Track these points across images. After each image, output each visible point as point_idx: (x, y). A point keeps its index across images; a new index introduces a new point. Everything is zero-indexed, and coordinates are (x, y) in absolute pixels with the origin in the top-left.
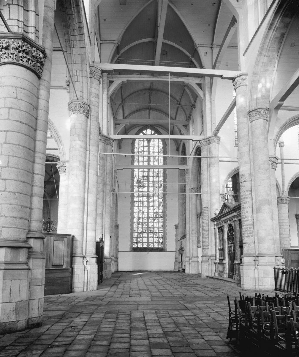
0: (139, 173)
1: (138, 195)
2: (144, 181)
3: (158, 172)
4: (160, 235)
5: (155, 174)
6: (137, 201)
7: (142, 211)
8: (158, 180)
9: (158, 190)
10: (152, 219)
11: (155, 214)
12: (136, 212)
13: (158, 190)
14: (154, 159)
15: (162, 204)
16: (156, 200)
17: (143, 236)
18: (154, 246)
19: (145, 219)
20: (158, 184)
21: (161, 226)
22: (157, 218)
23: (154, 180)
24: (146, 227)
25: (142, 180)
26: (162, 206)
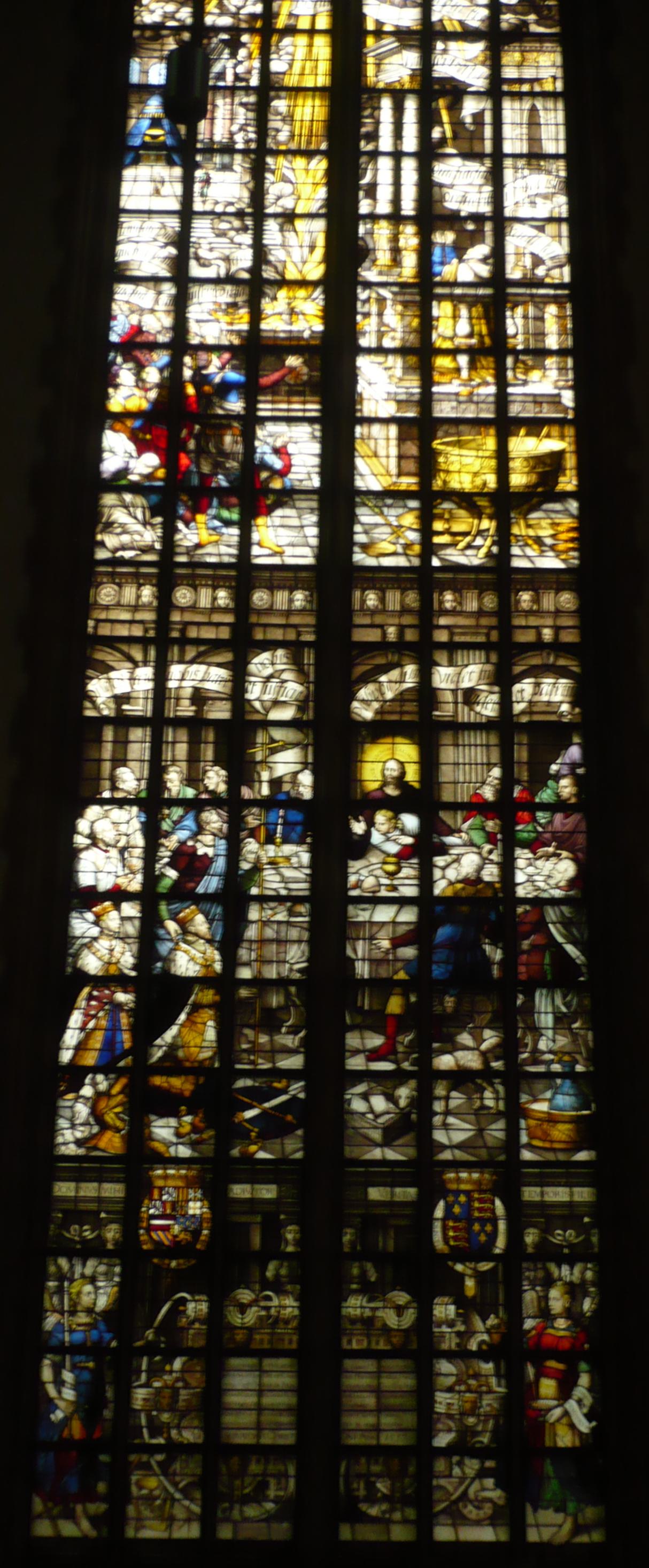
0: (180, 304)
1: (163, 622)
2: (265, 408)
3: (498, 279)
4: (557, 1300)
5: (442, 310)
6: (138, 707)
7: (210, 884)
8: (502, 399)
9: (504, 538)
10: (395, 1005)
11: (443, 932)
12: (117, 896)
13: (504, 538)
14: (427, 120)
15: (574, 752)
16: (470, 697)
17: (215, 1318)
18: (425, 1524)
19: (271, 1022)
20: (502, 458)
21: (562, 1132)
22: (488, 1006)
23: (426, 400)
24: (293, 1147)
25: (235, 404)
26: (566, 787)
